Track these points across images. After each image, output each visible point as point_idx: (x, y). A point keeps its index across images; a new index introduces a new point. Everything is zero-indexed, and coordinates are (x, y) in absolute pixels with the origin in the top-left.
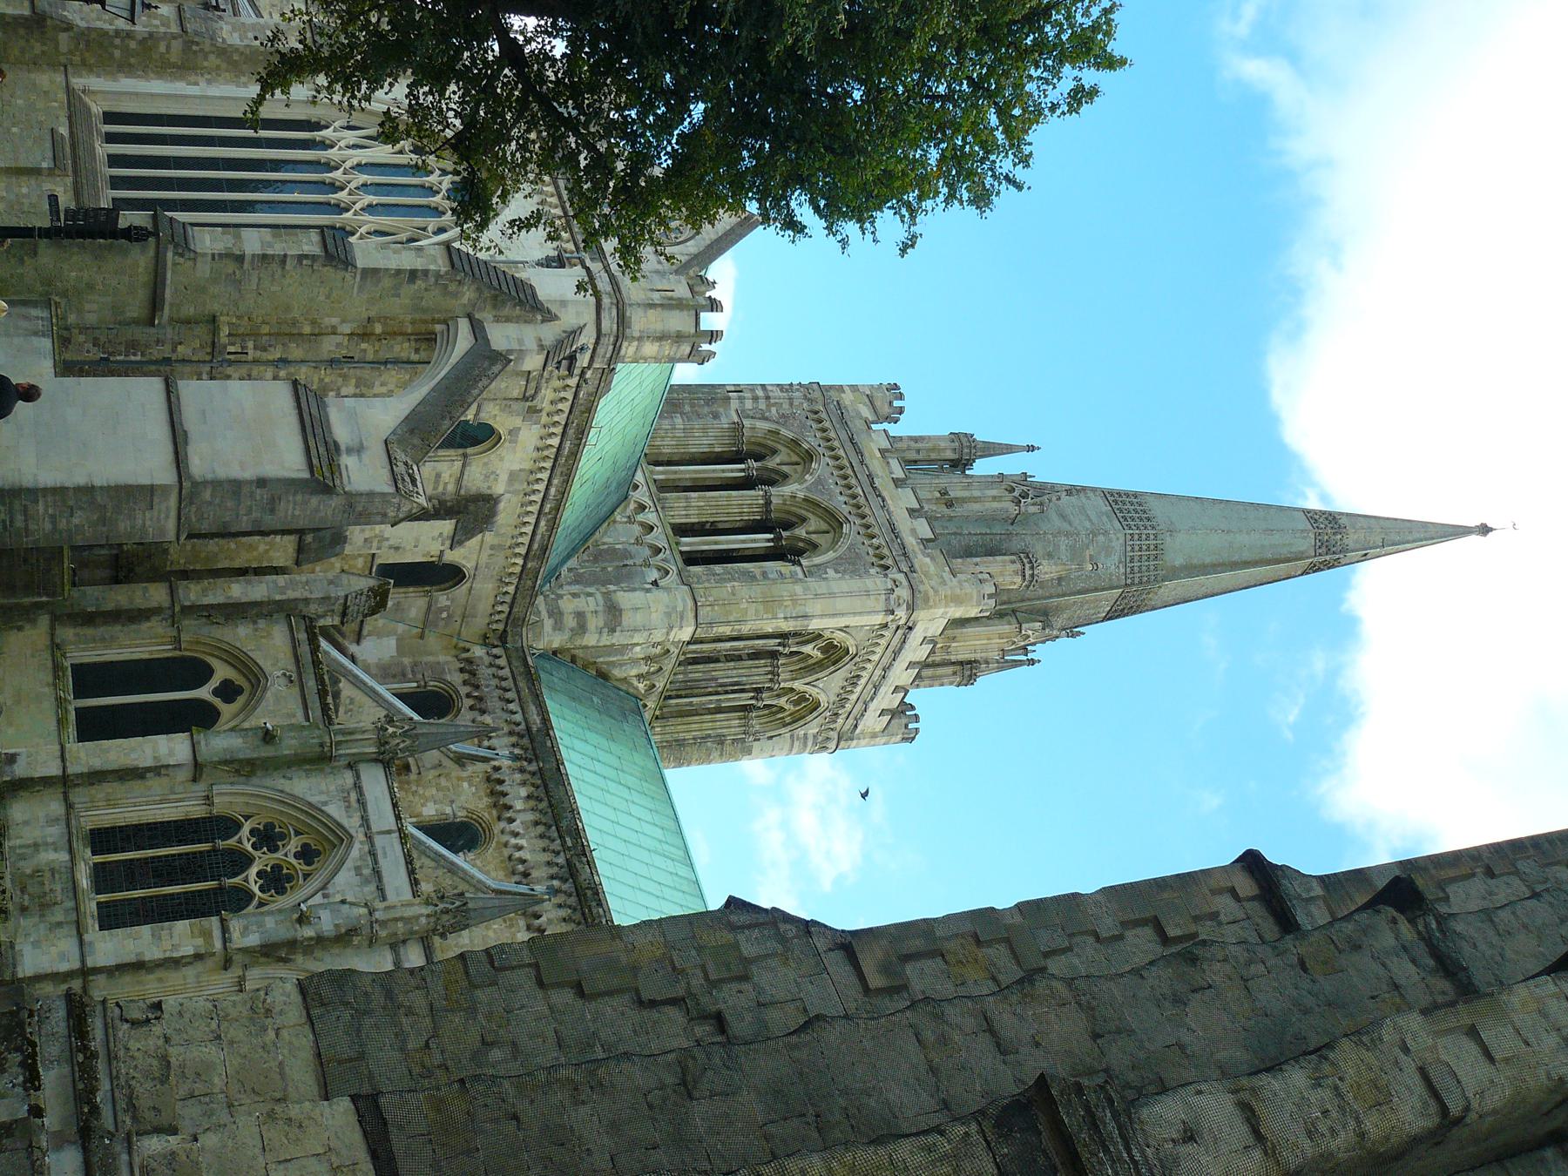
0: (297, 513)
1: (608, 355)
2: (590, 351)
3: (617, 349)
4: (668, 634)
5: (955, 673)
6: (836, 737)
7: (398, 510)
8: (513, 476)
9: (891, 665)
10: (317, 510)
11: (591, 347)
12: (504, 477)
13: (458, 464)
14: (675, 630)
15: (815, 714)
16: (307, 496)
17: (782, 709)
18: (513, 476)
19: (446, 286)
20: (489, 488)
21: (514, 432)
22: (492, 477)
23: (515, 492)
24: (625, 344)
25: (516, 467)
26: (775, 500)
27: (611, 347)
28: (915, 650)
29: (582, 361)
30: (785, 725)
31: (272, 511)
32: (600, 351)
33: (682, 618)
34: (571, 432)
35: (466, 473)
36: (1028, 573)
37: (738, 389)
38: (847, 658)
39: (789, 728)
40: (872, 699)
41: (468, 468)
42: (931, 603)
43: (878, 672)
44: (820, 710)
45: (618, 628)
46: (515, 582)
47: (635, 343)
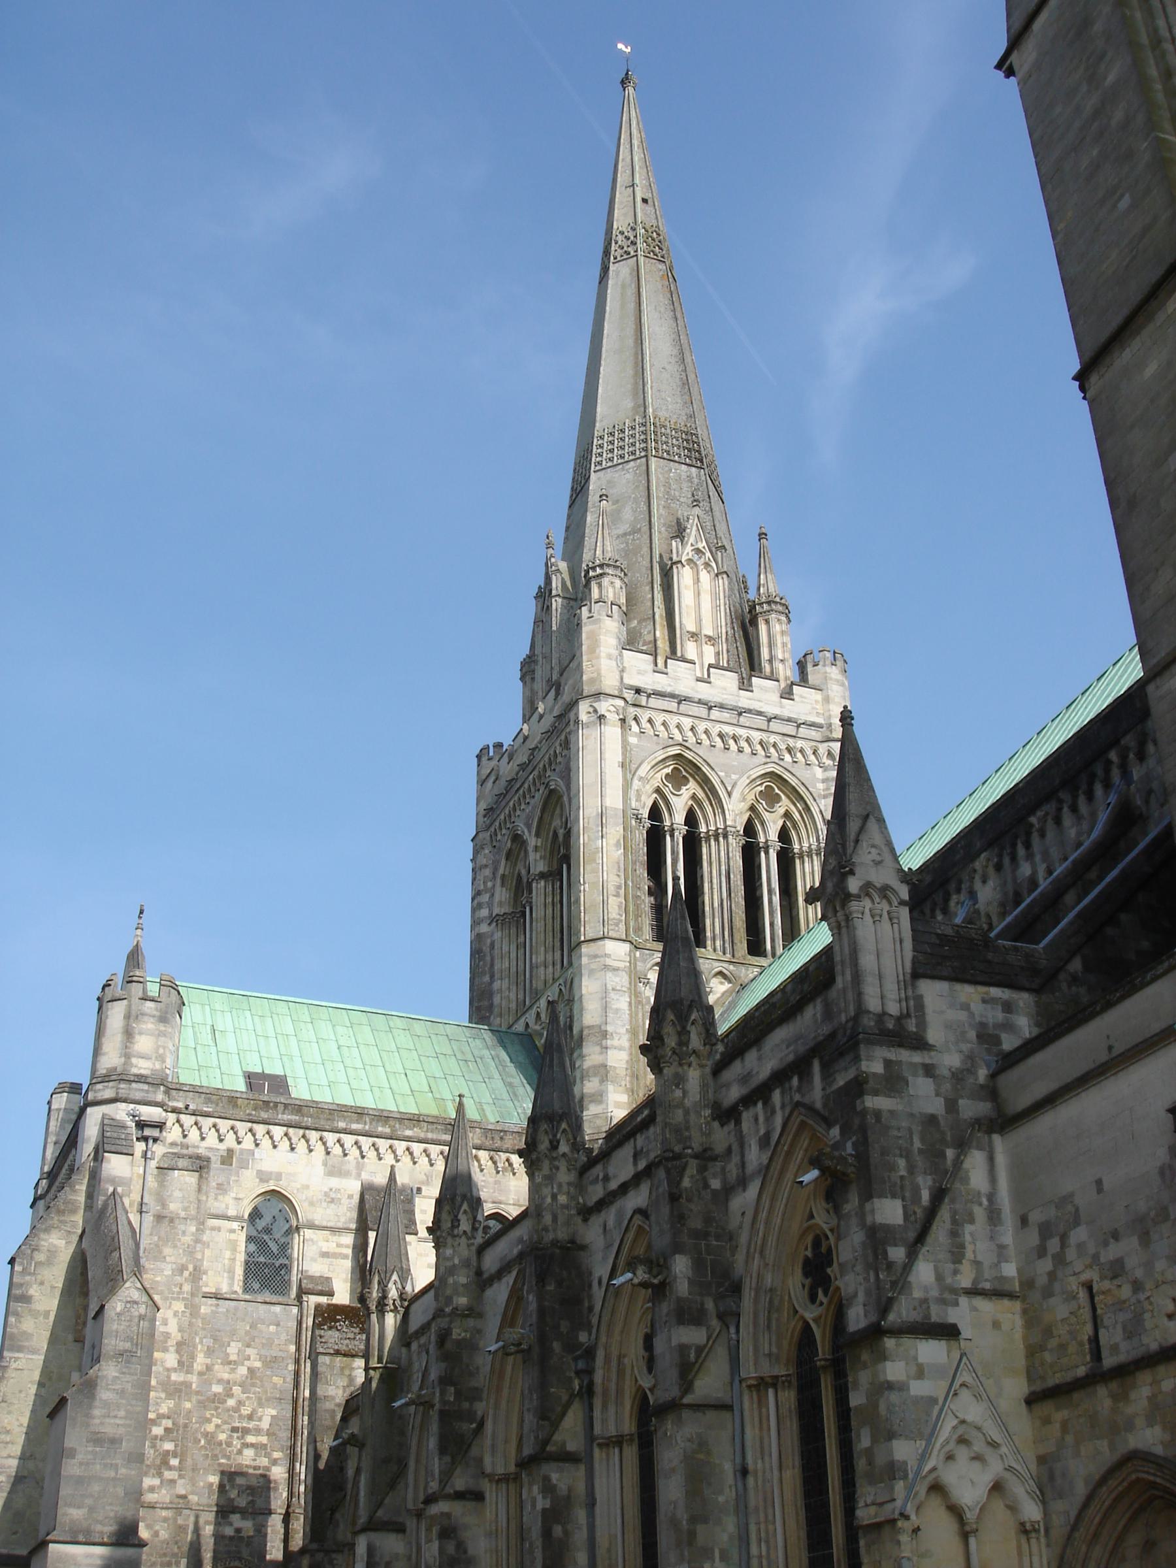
0: (122, 1413)
1: (146, 1087)
2: (138, 1107)
3: (141, 1079)
4: (616, 969)
5: (767, 622)
6: (826, 744)
7: (136, 1303)
8: (333, 1171)
9: (700, 702)
10: (122, 1393)
11: (132, 1106)
12: (334, 1182)
13: (308, 1233)
14: (609, 962)
15: (787, 776)
16: (97, 1403)
17: (787, 815)
18: (333, 1171)
19: (38, 1264)
20: (350, 1197)
21: (263, 1177)
22: (333, 1195)
23: (360, 1168)
24: (135, 1071)
25: (320, 1170)
26: (540, 867)
27: (134, 1085)
28: (677, 679)
29: (150, 1113)
30: (807, 808)
31: (114, 1441)
32: (138, 1096)
33: (596, 956)
34: (264, 1115)
35: (324, 1224)
36: (599, 571)
37: (475, 923)
38: (688, 755)
39: (810, 802)
40: (760, 713)
41: (317, 1223)
42: (595, 675)
43: (715, 714)
44: (779, 770)
45: (603, 1028)
46: (504, 1156)
47: (134, 1060)
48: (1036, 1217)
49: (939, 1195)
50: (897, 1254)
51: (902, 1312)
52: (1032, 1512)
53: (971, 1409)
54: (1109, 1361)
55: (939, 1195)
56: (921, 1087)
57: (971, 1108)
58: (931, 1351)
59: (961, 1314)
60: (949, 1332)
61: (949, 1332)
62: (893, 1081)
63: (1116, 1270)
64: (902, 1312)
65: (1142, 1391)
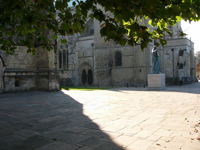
48: (80, 47)
49: (75, 45)
50: (73, 49)
51: (73, 52)
52: (78, 64)
53: (76, 58)
54: (84, 56)
55: (75, 45)
56: (74, 38)
57: (77, 40)
58: (74, 55)
59: (75, 53)
60: (75, 54)
61: (75, 54)
62: (73, 38)
63: (86, 51)
64: (73, 52)
65: (86, 58)
